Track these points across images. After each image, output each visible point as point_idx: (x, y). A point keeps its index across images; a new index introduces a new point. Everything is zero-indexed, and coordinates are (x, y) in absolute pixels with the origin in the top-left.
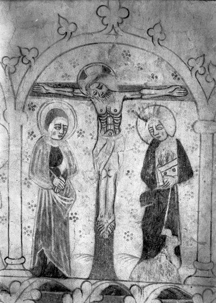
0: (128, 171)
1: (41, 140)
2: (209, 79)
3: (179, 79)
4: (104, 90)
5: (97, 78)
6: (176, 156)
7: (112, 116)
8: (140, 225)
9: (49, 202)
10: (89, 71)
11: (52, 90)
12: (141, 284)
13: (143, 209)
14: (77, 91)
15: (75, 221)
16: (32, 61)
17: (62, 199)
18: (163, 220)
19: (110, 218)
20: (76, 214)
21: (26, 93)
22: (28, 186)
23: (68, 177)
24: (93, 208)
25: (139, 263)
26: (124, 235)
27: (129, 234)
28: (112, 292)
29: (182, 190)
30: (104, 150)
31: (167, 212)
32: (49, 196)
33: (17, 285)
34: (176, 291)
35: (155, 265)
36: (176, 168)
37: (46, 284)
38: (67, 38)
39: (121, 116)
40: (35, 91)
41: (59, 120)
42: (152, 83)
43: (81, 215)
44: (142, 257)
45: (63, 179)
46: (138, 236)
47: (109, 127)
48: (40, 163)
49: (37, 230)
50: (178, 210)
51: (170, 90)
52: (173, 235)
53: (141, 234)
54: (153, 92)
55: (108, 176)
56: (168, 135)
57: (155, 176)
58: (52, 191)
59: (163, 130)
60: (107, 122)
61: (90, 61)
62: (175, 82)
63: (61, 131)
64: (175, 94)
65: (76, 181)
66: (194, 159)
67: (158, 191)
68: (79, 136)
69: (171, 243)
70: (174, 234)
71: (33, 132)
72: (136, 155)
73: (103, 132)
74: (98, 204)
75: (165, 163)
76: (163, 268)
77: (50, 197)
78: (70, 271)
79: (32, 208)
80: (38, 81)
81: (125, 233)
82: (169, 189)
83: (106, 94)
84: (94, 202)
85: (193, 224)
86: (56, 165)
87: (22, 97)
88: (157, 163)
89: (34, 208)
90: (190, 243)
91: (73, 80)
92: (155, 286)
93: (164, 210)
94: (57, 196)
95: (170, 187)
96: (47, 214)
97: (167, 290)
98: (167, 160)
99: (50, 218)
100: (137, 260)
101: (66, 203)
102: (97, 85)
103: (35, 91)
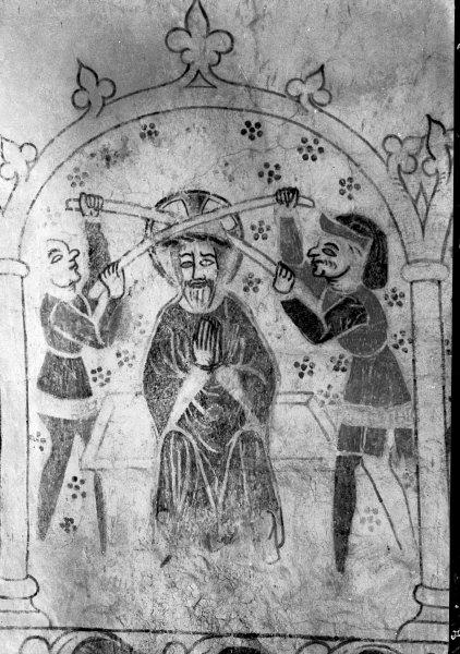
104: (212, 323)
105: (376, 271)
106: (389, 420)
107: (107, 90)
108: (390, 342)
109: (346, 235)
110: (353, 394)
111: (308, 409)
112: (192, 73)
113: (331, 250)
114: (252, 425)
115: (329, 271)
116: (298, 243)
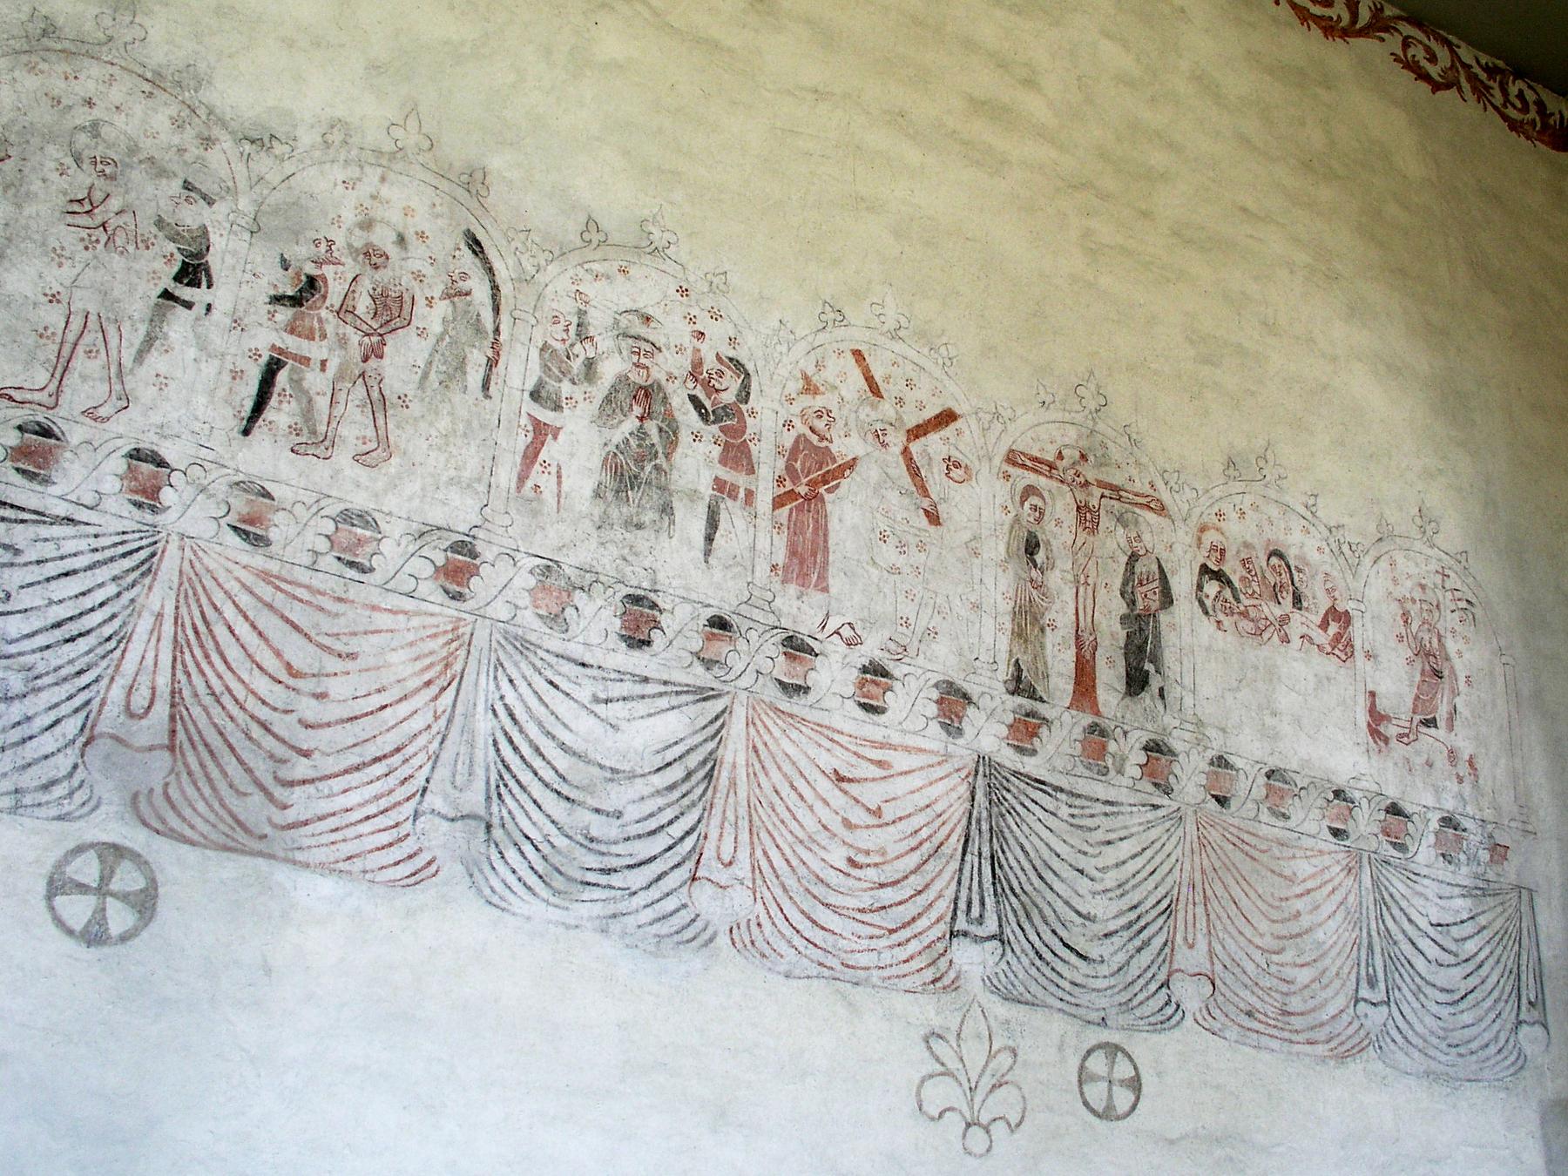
37: (1020, 706)
60: (1086, 516)
69: (1155, 682)
72: (1115, 566)
78: (1047, 690)
86: (1032, 554)
94: (1035, 592)
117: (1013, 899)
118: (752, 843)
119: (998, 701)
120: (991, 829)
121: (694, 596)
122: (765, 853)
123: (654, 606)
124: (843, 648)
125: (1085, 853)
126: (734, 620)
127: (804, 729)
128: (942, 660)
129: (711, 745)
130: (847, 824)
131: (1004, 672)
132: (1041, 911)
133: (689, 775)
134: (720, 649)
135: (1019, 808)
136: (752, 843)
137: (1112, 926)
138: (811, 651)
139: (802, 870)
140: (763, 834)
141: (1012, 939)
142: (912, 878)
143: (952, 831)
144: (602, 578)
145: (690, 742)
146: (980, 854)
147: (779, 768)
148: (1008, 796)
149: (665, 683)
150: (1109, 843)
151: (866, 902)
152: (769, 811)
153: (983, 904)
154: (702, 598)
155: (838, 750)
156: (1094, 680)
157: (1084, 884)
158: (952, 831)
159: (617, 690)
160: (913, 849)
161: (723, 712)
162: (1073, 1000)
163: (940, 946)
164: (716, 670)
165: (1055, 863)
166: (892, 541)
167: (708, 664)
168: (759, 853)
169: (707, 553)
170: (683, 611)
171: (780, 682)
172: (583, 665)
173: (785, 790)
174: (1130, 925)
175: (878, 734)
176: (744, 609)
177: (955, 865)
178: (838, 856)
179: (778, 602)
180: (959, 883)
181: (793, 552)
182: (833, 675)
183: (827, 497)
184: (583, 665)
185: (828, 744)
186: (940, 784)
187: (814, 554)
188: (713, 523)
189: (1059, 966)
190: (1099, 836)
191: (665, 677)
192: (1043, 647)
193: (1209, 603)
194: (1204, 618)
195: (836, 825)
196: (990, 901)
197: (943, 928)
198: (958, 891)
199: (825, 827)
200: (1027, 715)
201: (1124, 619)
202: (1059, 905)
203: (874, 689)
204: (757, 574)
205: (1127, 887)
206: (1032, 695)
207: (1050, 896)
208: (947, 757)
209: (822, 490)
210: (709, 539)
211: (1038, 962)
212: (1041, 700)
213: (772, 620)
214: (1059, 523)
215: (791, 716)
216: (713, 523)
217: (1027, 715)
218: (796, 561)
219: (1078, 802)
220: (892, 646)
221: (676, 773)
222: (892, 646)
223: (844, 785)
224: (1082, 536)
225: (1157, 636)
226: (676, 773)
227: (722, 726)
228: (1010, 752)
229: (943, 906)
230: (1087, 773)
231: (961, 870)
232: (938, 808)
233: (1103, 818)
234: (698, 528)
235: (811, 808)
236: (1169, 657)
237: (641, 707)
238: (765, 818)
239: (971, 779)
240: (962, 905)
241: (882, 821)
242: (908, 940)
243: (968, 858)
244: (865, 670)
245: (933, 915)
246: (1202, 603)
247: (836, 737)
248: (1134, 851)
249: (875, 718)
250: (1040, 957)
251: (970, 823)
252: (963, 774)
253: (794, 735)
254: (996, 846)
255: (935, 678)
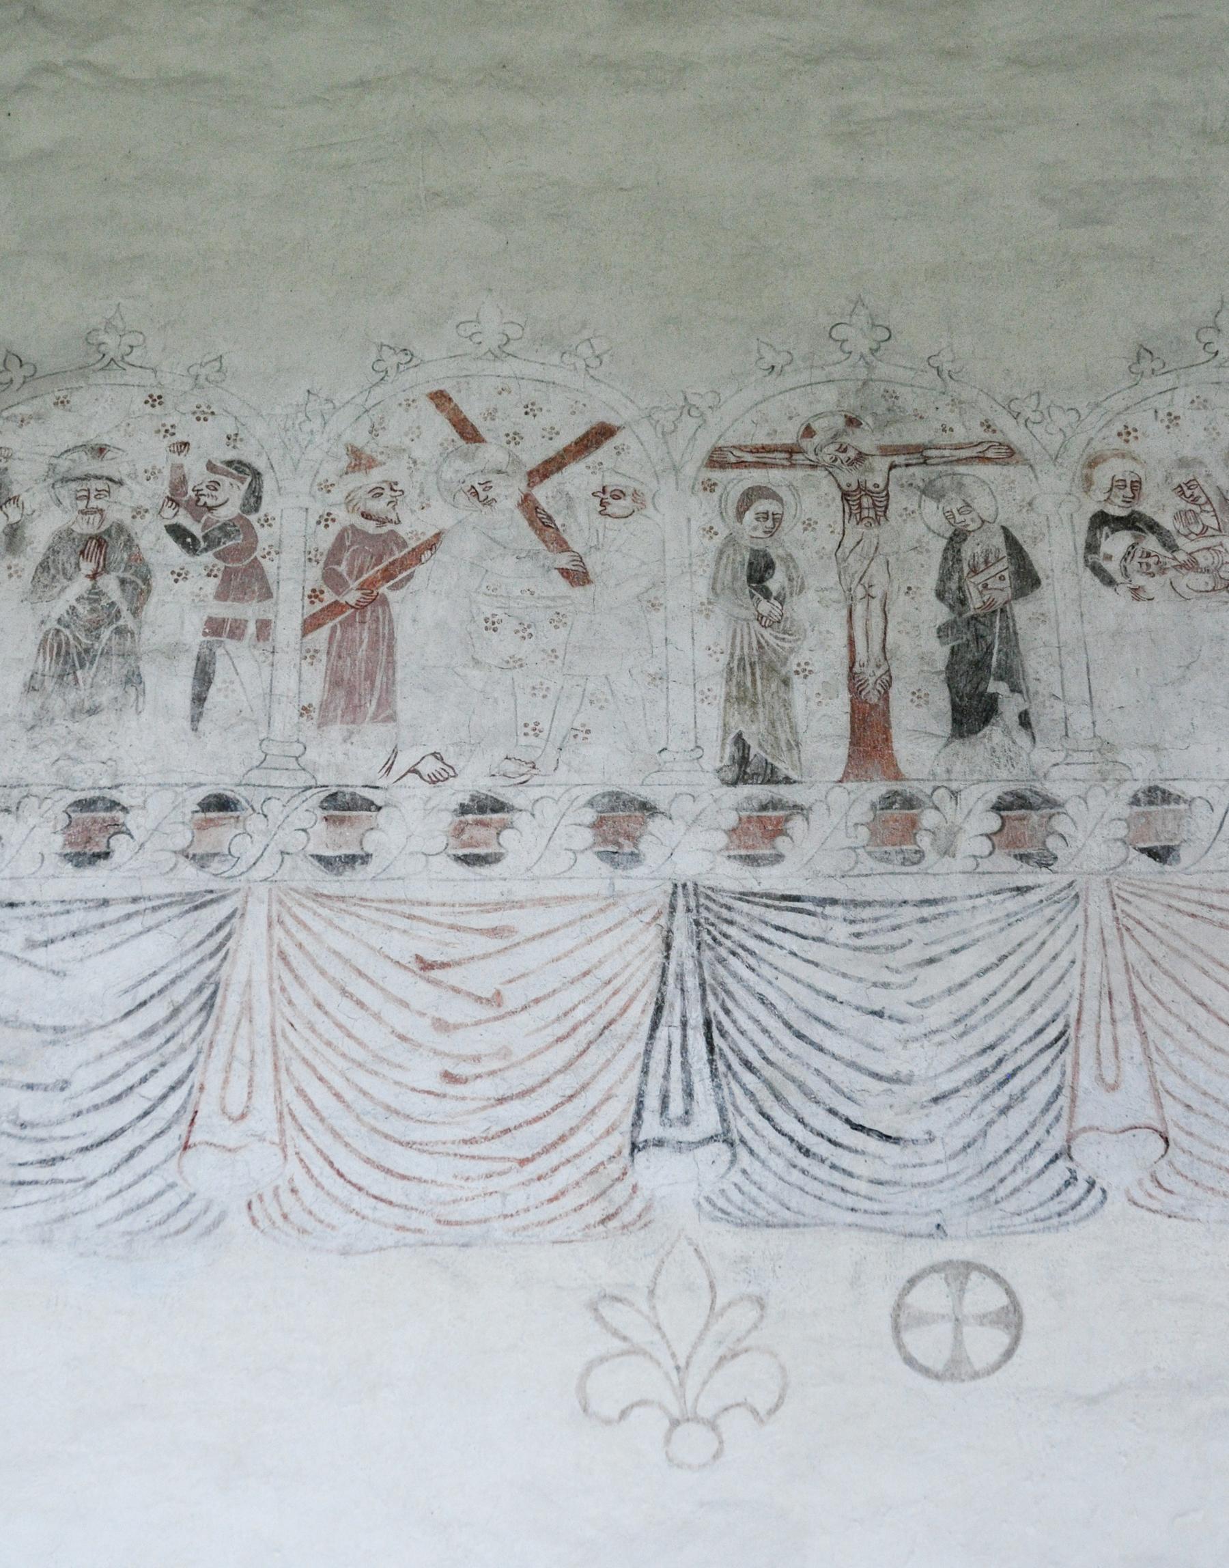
0: (909, 588)
1: (731, 540)
2: (1051, 428)
3: (994, 431)
4: (852, 454)
5: (835, 436)
6: (1004, 553)
7: (869, 493)
8: (943, 676)
9: (750, 644)
10: (815, 426)
11: (749, 458)
12: (954, 786)
13: (946, 650)
14: (795, 457)
15: (806, 677)
16: (709, 412)
17: (776, 637)
18: (989, 667)
19: (878, 666)
20: (807, 664)
21: (699, 464)
22: (707, 616)
23: (788, 600)
24: (845, 652)
25: (946, 746)
26: (911, 697)
27: (922, 694)
28: (893, 803)
29: (1022, 611)
30: (858, 549)
31: (995, 651)
32: (749, 634)
33: (687, 803)
34: (1028, 793)
35: (980, 748)
36: (1006, 574)
37: (749, 799)
38: (774, 375)
39: (887, 495)
40: (717, 460)
41: (763, 505)
42: (943, 439)
43: (816, 664)
44: (952, 736)
45: (777, 603)
46: (942, 700)
47: (865, 513)
48: (729, 578)
49: (728, 694)
50: (1017, 645)
51: (979, 449)
52: (1012, 691)
53: (947, 693)
54: (946, 453)
55: (869, 596)
56: (983, 522)
57: (963, 592)
58: (756, 623)
59: (974, 515)
61: (819, 408)
62: (987, 436)
63: (769, 523)
64: (990, 454)
65: (803, 608)
66: (1039, 558)
67: (972, 617)
68: (805, 529)
69: (1010, 707)
70: (1015, 689)
71: (711, 528)
72: (922, 558)
73: (854, 522)
74: (851, 642)
75: (983, 567)
76: (999, 753)
77: (753, 634)
79: (715, 656)
80: (721, 443)
81: (914, 693)
82: (994, 612)
83: (856, 459)
84: (845, 641)
85: (1052, 669)
86: (761, 580)
87: (690, 470)
88: (966, 570)
89: (719, 655)
90: (1047, 704)
91: (788, 439)
92: (983, 787)
93: (990, 647)
94: (767, 633)
95: (998, 606)
96: (748, 667)
97: (1011, 793)
98: (986, 562)
99: (753, 674)
100: (944, 741)
101: (787, 645)
102: (837, 446)
103: (717, 460)
104: (100, 542)
105: (254, 499)
106: (250, 611)
107: (27, 370)
108: (258, 554)
109: (228, 474)
110: (222, 595)
111: (181, 601)
112: (106, 360)
113: (214, 486)
114: (127, 620)
115: (210, 502)
116: (184, 481)
117: (747, 1077)
118: (277, 1081)
119: (706, 801)
120: (702, 985)
121: (175, 778)
122: (300, 1092)
123: (114, 805)
124: (425, 789)
125: (886, 985)
126: (241, 794)
127: (362, 912)
128: (605, 765)
129: (211, 965)
130: (441, 1026)
131: (717, 754)
132: (801, 1086)
133: (176, 1011)
134: (224, 834)
135: (752, 943)
136: (277, 1081)
137: (945, 1085)
138: (369, 805)
139: (361, 1104)
140: (298, 1068)
141: (748, 1134)
142: (559, 1080)
143: (632, 1000)
144: (34, 790)
145: (176, 968)
146: (684, 1024)
147: (323, 973)
148: (731, 931)
149: (135, 900)
150: (931, 961)
151: (476, 1127)
152: (308, 1034)
153: (689, 1094)
154: (188, 777)
155: (422, 929)
156: (886, 730)
157: (884, 1031)
158: (632, 1000)
159: (62, 925)
160: (559, 1040)
161: (230, 918)
162: (876, 1207)
163: (614, 1169)
164: (215, 866)
165: (827, 1011)
166: (508, 626)
167: (201, 861)
168: (289, 1093)
169: (195, 719)
170: (159, 803)
171: (320, 858)
172: (11, 905)
173: (333, 1001)
174: (983, 1075)
175: (492, 892)
176: (255, 777)
177: (639, 1046)
178: (425, 1073)
179: (311, 754)
180: (645, 1071)
181: (336, 681)
182: (411, 828)
183: (392, 596)
184: (11, 905)
185: (402, 923)
186: (607, 939)
187: (370, 677)
188: (204, 676)
189: (845, 1160)
190: (913, 953)
191: (135, 892)
192: (787, 705)
193: (1112, 567)
194: (1107, 592)
195: (420, 1030)
196: (703, 1086)
197: (620, 1140)
198: (644, 1082)
199: (403, 1038)
200: (764, 808)
201: (942, 632)
202: (838, 1072)
203: (479, 833)
204: (278, 724)
205: (971, 1021)
206: (771, 776)
207: (817, 1060)
208: (615, 898)
209: (384, 589)
210: (199, 699)
211: (803, 1161)
212: (788, 780)
213: (303, 779)
214: (809, 525)
215: (342, 899)
216: (204, 676)
217: (764, 808)
218: (341, 693)
219: (867, 913)
220: (511, 767)
221: (157, 1011)
222: (511, 767)
223: (435, 974)
224: (855, 531)
225: (1011, 638)
226: (157, 1011)
227: (229, 937)
228: (734, 868)
229: (619, 1109)
230: (882, 867)
231: (648, 1052)
232: (605, 972)
233: (919, 928)
234: (181, 688)
235: (377, 1016)
236: (1037, 664)
237: (101, 939)
238: (299, 1044)
239: (663, 921)
240: (652, 1102)
241: (502, 1011)
242: (555, 1170)
243: (662, 1032)
244: (464, 810)
245: (599, 1125)
246: (1097, 570)
247: (417, 911)
248: (984, 963)
249: (485, 871)
250: (807, 1153)
251: (663, 982)
252: (647, 916)
253: (348, 923)
254: (713, 1006)
255: (586, 794)
